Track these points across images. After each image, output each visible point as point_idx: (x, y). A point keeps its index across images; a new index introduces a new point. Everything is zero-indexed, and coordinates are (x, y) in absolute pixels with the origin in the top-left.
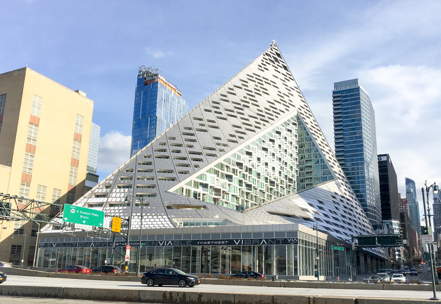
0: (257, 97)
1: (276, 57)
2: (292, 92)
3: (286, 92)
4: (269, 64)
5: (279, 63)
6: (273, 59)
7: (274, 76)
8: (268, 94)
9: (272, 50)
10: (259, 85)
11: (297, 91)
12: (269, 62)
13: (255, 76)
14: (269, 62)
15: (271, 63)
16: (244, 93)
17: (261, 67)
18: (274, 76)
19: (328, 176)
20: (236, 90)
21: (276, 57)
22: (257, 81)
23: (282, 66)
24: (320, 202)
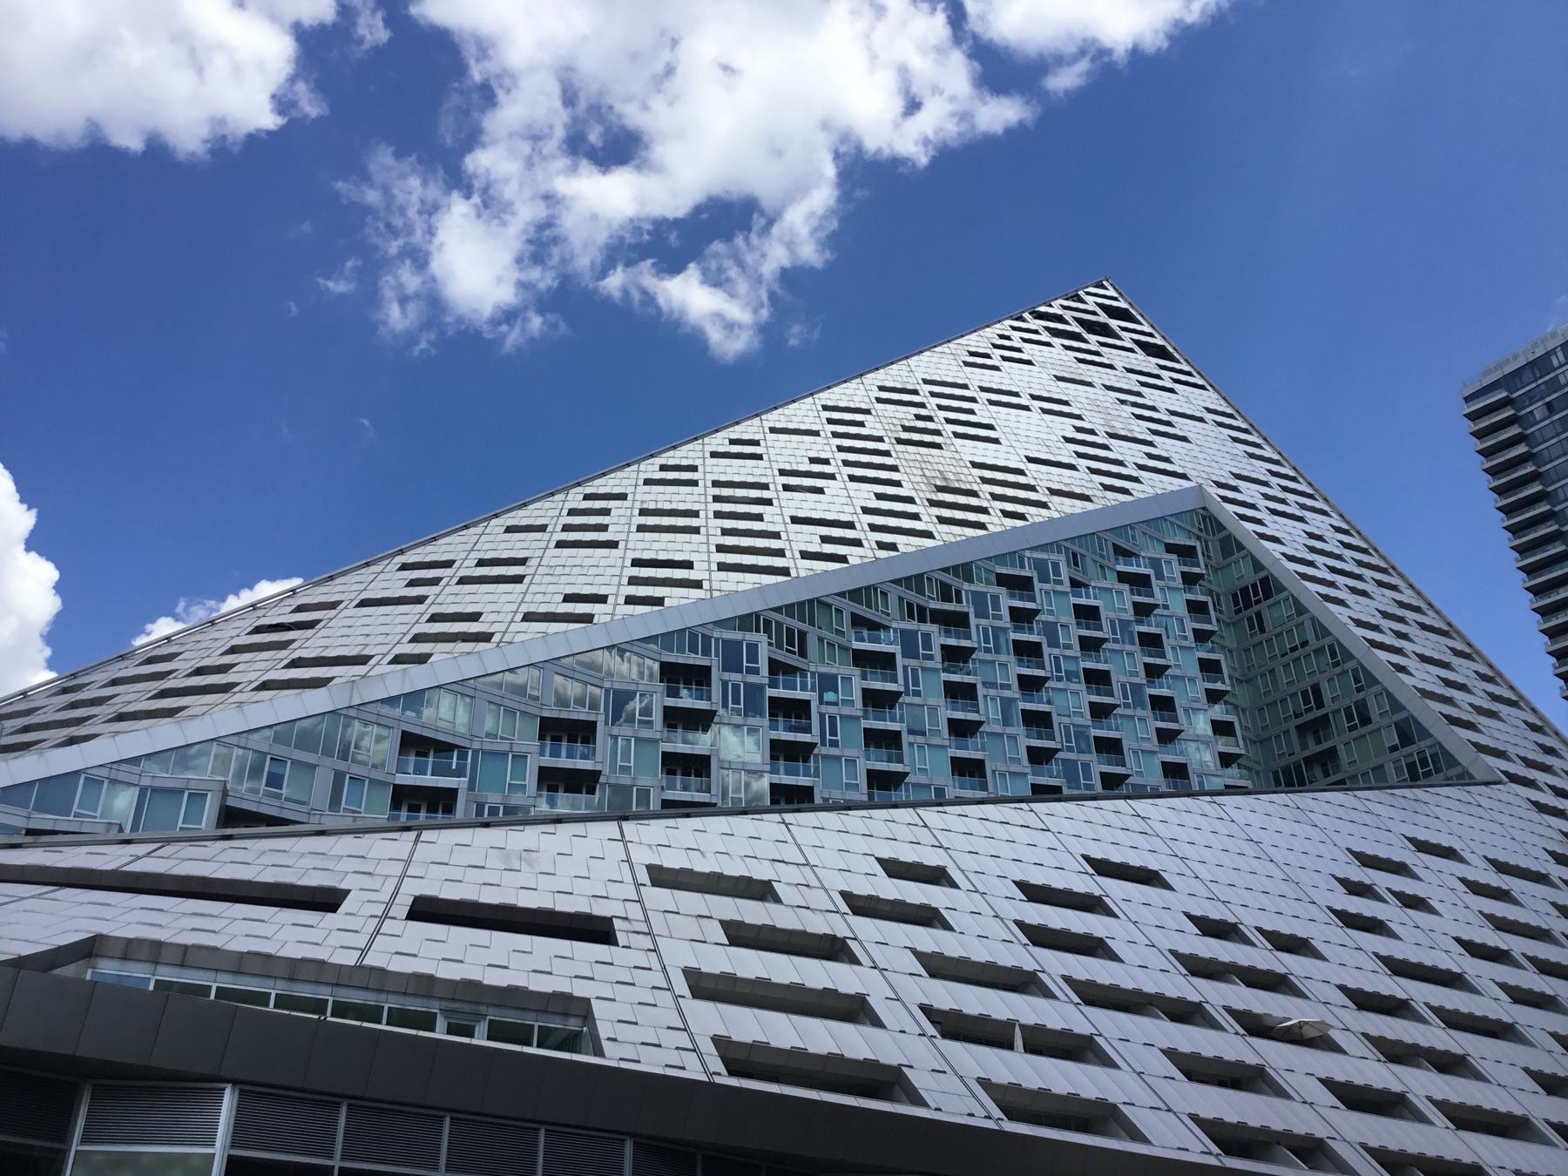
1: (1103, 318)
3: (1140, 429)
6: (1075, 328)
7: (1059, 379)
8: (996, 441)
12: (1045, 337)
14: (1045, 337)
15: (1057, 341)
18: (1059, 379)
21: (1103, 318)
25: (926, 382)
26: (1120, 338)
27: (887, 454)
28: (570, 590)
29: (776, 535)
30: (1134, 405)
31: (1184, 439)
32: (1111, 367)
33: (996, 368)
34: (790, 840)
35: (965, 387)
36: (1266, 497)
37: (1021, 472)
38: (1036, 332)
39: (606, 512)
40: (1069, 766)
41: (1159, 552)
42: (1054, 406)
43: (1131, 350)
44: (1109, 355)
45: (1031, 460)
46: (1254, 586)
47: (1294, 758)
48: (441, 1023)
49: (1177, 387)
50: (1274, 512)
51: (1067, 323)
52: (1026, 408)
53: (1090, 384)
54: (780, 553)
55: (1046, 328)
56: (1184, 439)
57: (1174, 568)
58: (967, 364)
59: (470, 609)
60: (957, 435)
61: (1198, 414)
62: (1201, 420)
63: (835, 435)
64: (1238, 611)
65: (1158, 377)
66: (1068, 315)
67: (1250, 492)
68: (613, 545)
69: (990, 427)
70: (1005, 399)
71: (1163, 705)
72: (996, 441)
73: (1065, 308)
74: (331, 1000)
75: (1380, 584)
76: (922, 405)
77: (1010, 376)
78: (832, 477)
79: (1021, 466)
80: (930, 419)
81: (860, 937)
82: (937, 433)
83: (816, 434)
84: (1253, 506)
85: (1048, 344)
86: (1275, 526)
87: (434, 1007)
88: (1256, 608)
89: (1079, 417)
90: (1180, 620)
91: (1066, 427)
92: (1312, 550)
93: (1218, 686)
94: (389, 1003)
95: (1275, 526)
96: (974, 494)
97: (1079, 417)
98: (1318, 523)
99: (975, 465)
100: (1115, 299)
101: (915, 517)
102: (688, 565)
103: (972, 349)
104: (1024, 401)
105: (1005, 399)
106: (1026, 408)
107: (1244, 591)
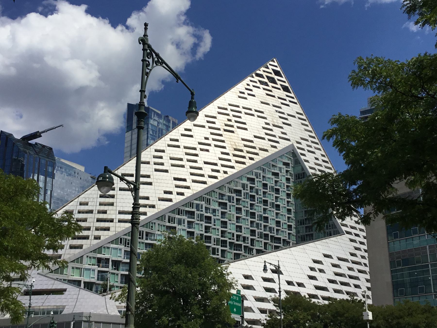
1: (273, 75)
2: (291, 120)
3: (280, 122)
4: (259, 88)
5: (276, 83)
6: (266, 80)
7: (262, 103)
8: (246, 129)
9: (267, 68)
10: (234, 119)
11: (299, 118)
12: (258, 84)
13: (230, 108)
15: (262, 86)
16: (206, 132)
17: (243, 93)
18: (262, 103)
19: (332, 231)
20: (196, 131)
21: (273, 75)
22: (231, 113)
23: (279, 86)
24: (247, 277)
25: (230, 105)
27: (221, 135)
30: (280, 112)
32: (274, 96)
33: (245, 98)
35: (238, 106)
37: (252, 141)
38: (256, 82)
41: (281, 165)
45: (255, 137)
46: (301, 174)
47: (303, 218)
53: (268, 104)
54: (202, 176)
55: (260, 81)
57: (284, 168)
58: (239, 97)
64: (296, 179)
68: (166, 171)
69: (244, 123)
71: (278, 207)
72: (246, 129)
73: (264, 71)
76: (228, 115)
85: (259, 88)
88: (301, 180)
89: (265, 118)
90: (284, 184)
93: (289, 200)
99: (243, 140)
107: (299, 174)
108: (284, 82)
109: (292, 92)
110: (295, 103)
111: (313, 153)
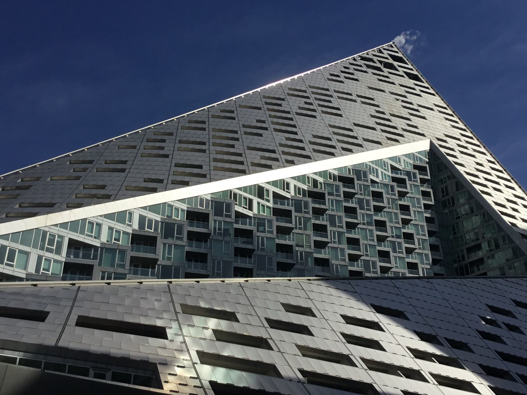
0: (299, 121)
1: (391, 61)
2: (423, 112)
3: (405, 113)
6: (378, 65)
8: (340, 115)
12: (364, 68)
14: (364, 68)
15: (370, 70)
21: (391, 61)
25: (310, 87)
26: (397, 70)
27: (291, 119)
28: (146, 176)
29: (240, 155)
30: (403, 101)
31: (424, 118)
32: (393, 83)
33: (342, 82)
34: (243, 294)
35: (327, 90)
36: (459, 145)
37: (351, 130)
38: (361, 66)
39: (164, 141)
40: (366, 262)
42: (368, 101)
43: (402, 76)
44: (393, 78)
45: (356, 125)
48: (92, 372)
49: (422, 94)
50: (462, 152)
51: (374, 62)
52: (355, 101)
53: (383, 91)
54: (242, 163)
56: (424, 118)
58: (329, 79)
59: (100, 183)
60: (323, 112)
61: (431, 107)
62: (432, 109)
63: (269, 110)
65: (414, 89)
66: (375, 59)
67: (452, 143)
68: (167, 156)
69: (338, 109)
70: (347, 97)
72: (340, 115)
74: (44, 361)
75: (507, 186)
76: (308, 98)
77: (348, 86)
78: (266, 129)
79: (351, 128)
80: (311, 104)
81: (273, 338)
82: (314, 111)
83: (260, 109)
84: (452, 150)
86: (462, 159)
87: (88, 365)
89: (378, 106)
91: (372, 110)
92: (478, 170)
94: (69, 363)
95: (462, 159)
96: (329, 139)
97: (378, 106)
98: (481, 158)
100: (397, 52)
101: (303, 149)
102: (200, 167)
103: (331, 73)
104: (353, 98)
105: (347, 97)
106: (355, 101)
108: (411, 69)
109: (425, 82)
110: (433, 95)
111: (473, 156)
